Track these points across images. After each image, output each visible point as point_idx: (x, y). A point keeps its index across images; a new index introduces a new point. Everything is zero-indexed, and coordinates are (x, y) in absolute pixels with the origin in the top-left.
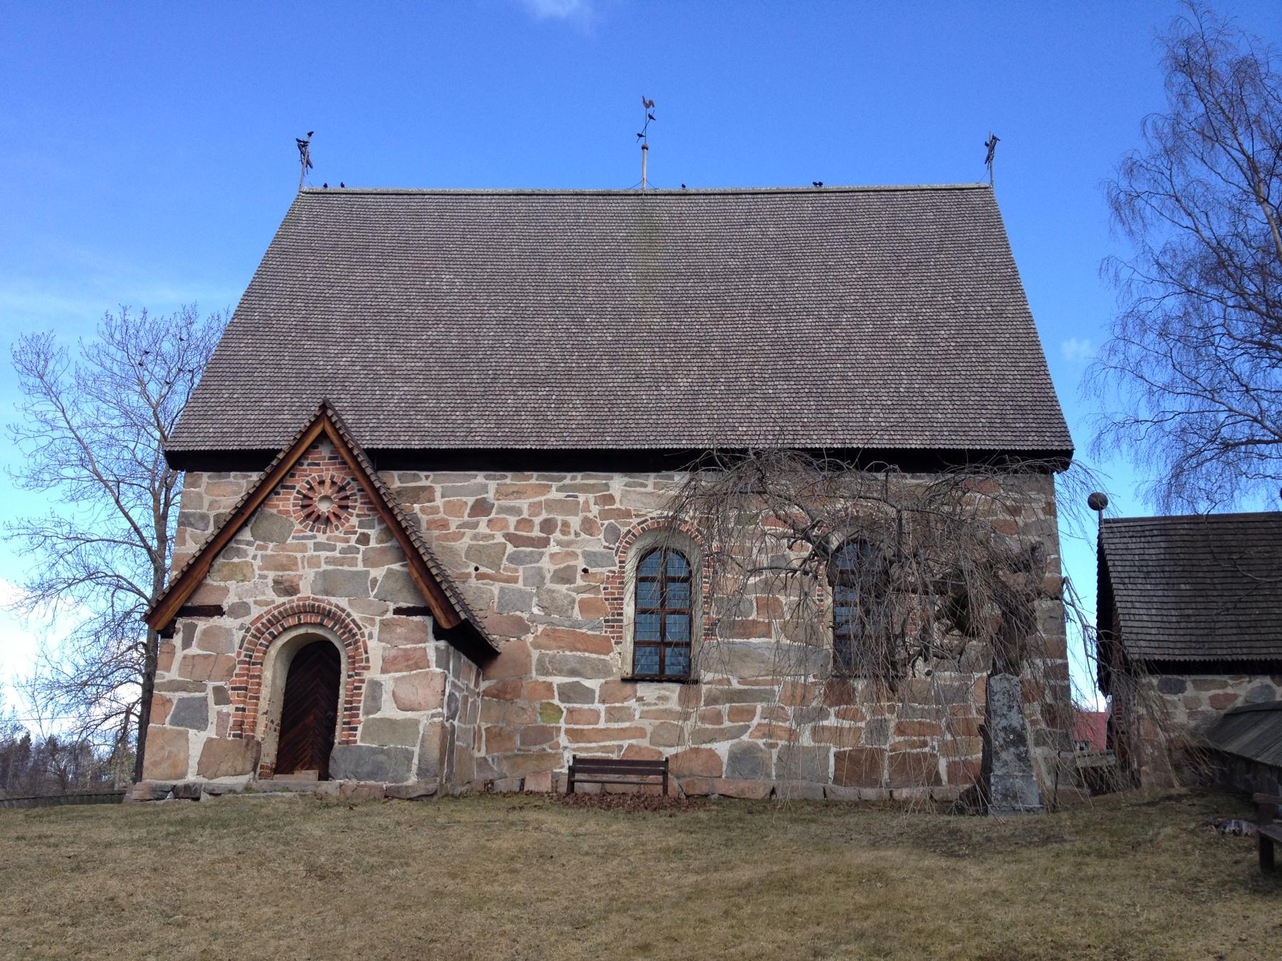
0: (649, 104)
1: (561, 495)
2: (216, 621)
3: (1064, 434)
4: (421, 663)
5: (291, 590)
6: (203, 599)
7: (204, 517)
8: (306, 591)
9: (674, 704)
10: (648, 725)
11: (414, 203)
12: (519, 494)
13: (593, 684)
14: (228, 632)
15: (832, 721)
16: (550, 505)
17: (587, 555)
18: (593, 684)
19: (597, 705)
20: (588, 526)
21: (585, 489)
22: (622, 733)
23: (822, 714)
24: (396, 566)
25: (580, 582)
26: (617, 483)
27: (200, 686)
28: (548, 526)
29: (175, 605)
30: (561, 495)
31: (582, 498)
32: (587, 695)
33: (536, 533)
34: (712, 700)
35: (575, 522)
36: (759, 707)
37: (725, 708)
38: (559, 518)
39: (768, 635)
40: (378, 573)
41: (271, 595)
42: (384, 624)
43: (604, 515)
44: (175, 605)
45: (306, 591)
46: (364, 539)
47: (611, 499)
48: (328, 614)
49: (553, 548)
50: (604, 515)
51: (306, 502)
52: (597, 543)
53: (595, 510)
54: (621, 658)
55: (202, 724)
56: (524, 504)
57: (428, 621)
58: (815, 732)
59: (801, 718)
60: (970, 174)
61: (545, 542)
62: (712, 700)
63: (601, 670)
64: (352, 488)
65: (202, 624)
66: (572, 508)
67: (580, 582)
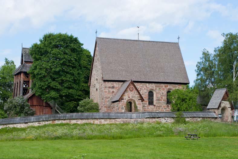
0: (138, 27)
1: (142, 86)
2: (123, 100)
3: (189, 81)
4: (140, 104)
5: (129, 97)
6: (123, 98)
7: (107, 87)
8: (131, 98)
9: (153, 107)
10: (151, 109)
11: (111, 40)
12: (138, 85)
13: (146, 105)
14: (124, 101)
15: (167, 109)
16: (141, 87)
17: (145, 92)
18: (146, 105)
19: (146, 107)
20: (145, 89)
21: (144, 85)
22: (149, 110)
23: (166, 108)
24: (138, 95)
25: (144, 95)
26: (147, 84)
27: (123, 106)
28: (141, 89)
29: (121, 98)
30: (142, 86)
31: (144, 86)
32: (145, 106)
33: (140, 90)
34: (157, 107)
35: (143, 88)
36: (161, 108)
37: (158, 108)
38: (142, 88)
39: (161, 101)
40: (136, 96)
41: (128, 98)
42: (137, 101)
43: (146, 88)
44: (121, 98)
45: (131, 98)
46: (135, 93)
47: (147, 86)
48: (132, 100)
49: (141, 91)
50: (146, 88)
51: (130, 89)
52: (146, 91)
53: (145, 87)
54: (148, 103)
55: (123, 109)
56: (138, 86)
57: (141, 100)
58: (166, 110)
59: (165, 109)
60: (176, 41)
61: (140, 91)
62: (157, 107)
63: (146, 104)
64: (134, 88)
65: (122, 100)
66: (143, 87)
67: (144, 95)
